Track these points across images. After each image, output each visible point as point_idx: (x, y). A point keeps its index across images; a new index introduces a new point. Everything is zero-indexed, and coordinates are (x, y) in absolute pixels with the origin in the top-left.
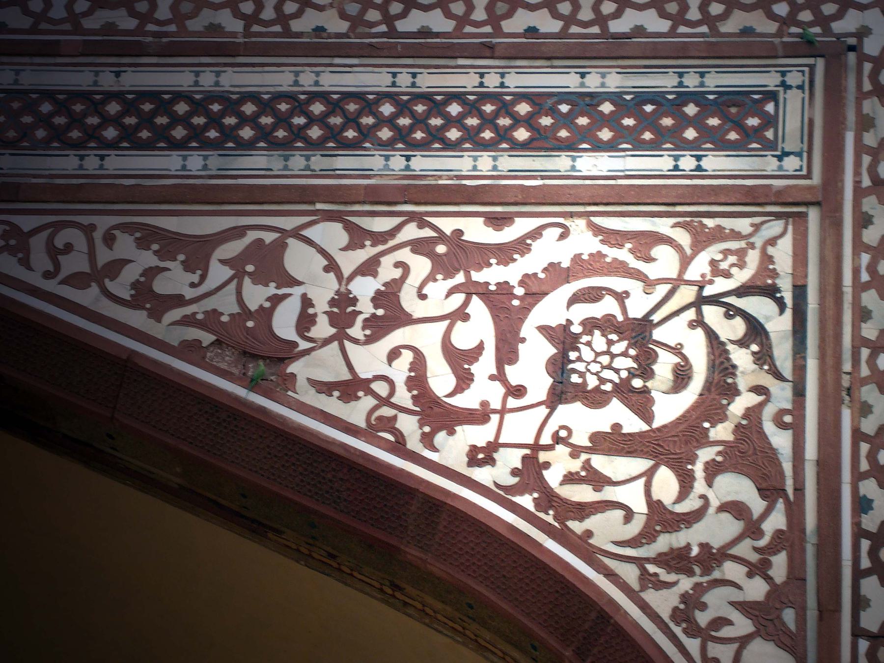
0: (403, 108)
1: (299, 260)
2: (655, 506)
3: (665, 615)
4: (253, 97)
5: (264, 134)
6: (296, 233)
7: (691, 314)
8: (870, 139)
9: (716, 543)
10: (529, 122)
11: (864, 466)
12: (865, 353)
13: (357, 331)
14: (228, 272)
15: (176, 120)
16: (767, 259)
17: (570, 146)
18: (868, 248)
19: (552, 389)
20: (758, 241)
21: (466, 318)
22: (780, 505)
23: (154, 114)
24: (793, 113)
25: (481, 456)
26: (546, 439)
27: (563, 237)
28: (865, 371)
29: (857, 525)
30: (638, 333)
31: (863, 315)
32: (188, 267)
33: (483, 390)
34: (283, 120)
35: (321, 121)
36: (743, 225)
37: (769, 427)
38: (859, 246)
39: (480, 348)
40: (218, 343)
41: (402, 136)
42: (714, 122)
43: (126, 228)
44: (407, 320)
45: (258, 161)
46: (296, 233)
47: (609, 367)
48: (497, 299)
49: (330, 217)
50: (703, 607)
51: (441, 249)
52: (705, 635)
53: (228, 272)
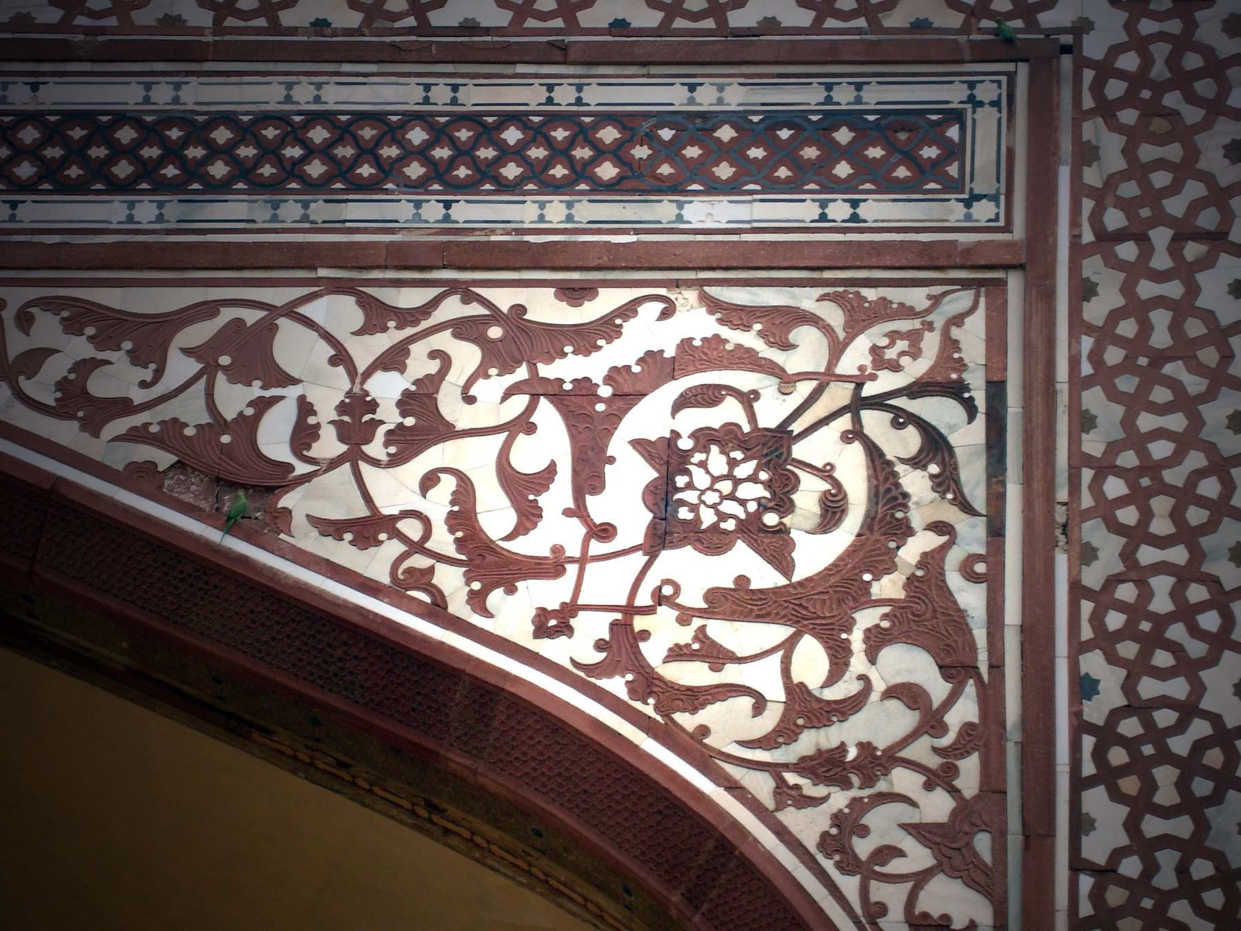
0: (440, 134)
1: (294, 348)
2: (796, 691)
3: (811, 843)
4: (228, 119)
5: (244, 172)
6: (290, 311)
7: (844, 422)
8: (1092, 176)
9: (881, 743)
10: (617, 153)
11: (1087, 633)
12: (1087, 475)
13: (376, 449)
14: (194, 366)
15: (118, 152)
16: (950, 344)
17: (675, 187)
18: (1090, 329)
19: (652, 527)
20: (938, 319)
21: (531, 429)
22: (970, 688)
23: (87, 142)
24: (985, 139)
25: (555, 623)
26: (644, 599)
27: (665, 314)
28: (1087, 501)
29: (1076, 715)
30: (772, 449)
31: (1083, 422)
32: (137, 359)
33: (556, 530)
34: (270, 152)
35: (325, 151)
36: (917, 297)
37: (954, 580)
38: (1078, 326)
39: (551, 470)
40: (180, 466)
41: (439, 174)
42: (875, 152)
43: (48, 304)
44: (448, 432)
45: (235, 208)
46: (290, 311)
47: (732, 497)
48: (575, 402)
49: (338, 287)
50: (864, 831)
51: (495, 332)
52: (866, 870)
53: (194, 366)
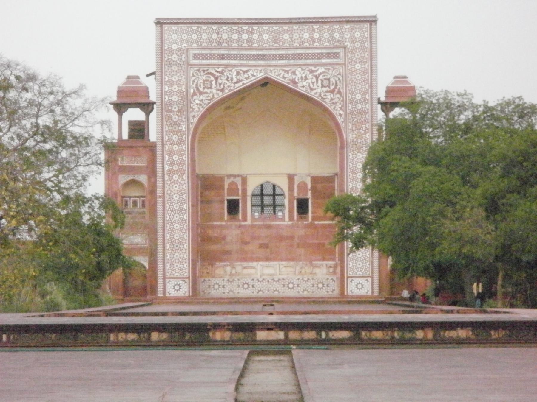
17: (321, 59)
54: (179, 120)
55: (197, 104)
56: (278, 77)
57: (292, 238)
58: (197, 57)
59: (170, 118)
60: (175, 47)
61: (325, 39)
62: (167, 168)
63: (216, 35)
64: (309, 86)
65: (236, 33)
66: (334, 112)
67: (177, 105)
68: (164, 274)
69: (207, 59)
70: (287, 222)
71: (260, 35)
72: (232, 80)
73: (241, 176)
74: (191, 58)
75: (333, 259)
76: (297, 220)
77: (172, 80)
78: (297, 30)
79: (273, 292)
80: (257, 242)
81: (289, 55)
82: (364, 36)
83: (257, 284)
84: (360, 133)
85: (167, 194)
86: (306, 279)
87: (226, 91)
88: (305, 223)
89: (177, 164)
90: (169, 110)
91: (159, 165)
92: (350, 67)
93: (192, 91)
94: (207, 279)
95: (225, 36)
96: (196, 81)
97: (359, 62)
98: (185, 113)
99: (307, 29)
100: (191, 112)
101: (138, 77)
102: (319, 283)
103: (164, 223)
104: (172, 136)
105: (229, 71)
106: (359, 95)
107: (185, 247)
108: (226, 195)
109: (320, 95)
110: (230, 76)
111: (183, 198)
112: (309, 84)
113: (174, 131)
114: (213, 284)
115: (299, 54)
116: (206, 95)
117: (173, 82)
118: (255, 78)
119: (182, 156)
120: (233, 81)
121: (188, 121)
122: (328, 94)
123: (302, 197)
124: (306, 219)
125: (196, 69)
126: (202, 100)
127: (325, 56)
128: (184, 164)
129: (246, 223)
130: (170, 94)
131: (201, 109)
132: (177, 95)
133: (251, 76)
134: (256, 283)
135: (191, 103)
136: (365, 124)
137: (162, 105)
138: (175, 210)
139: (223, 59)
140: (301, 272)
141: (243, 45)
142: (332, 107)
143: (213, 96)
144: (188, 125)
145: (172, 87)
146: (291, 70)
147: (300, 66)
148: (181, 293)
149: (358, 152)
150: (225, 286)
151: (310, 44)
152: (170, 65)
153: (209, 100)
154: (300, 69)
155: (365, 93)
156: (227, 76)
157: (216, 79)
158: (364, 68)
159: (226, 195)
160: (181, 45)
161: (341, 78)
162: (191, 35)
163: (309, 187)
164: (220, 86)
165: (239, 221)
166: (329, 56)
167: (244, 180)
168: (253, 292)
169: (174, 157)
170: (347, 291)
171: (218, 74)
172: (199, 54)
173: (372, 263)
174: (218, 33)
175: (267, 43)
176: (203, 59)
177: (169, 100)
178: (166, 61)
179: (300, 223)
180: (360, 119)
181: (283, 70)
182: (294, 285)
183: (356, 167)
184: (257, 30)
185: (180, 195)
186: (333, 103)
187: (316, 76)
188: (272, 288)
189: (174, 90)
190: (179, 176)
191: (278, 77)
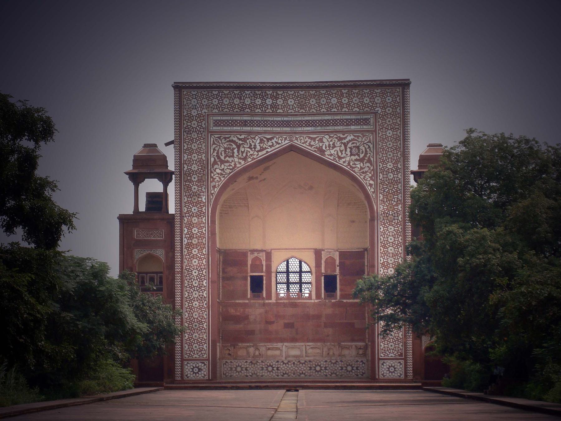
10: (346, 122)
17: (350, 125)
54: (198, 190)
55: (218, 174)
56: (304, 145)
57: (318, 317)
58: (218, 123)
59: (189, 188)
60: (194, 113)
61: (354, 104)
62: (185, 241)
63: (238, 100)
64: (337, 154)
65: (260, 98)
66: (364, 182)
67: (196, 174)
68: (182, 356)
69: (228, 126)
70: (314, 300)
71: (285, 100)
72: (255, 148)
73: (265, 251)
74: (212, 126)
75: (363, 340)
76: (325, 299)
77: (191, 148)
78: (325, 94)
79: (299, 376)
80: (282, 322)
81: (316, 121)
82: (396, 101)
83: (282, 366)
84: (392, 204)
85: (186, 269)
86: (333, 361)
87: (249, 160)
88: (333, 301)
89: (196, 237)
90: (188, 180)
91: (177, 238)
92: (380, 135)
93: (212, 159)
94: (229, 361)
95: (248, 101)
96: (217, 149)
97: (391, 129)
98: (205, 183)
99: (336, 94)
100: (211, 182)
101: (155, 146)
102: (347, 365)
103: (182, 300)
104: (191, 208)
105: (252, 138)
106: (391, 164)
107: (205, 326)
108: (249, 271)
109: (349, 164)
110: (253, 144)
111: (202, 274)
112: (337, 152)
113: (193, 203)
114: (235, 366)
115: (326, 120)
116: (227, 164)
117: (193, 150)
118: (280, 145)
119: (202, 229)
120: (256, 150)
121: (208, 192)
122: (357, 163)
123: (329, 273)
124: (334, 297)
125: (216, 136)
126: (223, 170)
127: (354, 122)
128: (204, 237)
129: (270, 301)
130: (190, 162)
131: (222, 179)
132: (196, 164)
133: (275, 144)
134: (282, 366)
135: (211, 172)
136: (397, 195)
137: (181, 175)
138: (194, 287)
139: (245, 125)
140: (328, 354)
141: (267, 111)
142: (362, 177)
143: (235, 164)
144: (208, 195)
145: (191, 155)
146: (318, 137)
147: (327, 133)
148: (200, 376)
149: (389, 225)
150: (248, 369)
151: (338, 110)
152: (189, 132)
153: (231, 169)
154: (327, 137)
155: (397, 162)
156: (250, 144)
157: (238, 147)
158: (396, 135)
159: (249, 271)
160: (201, 111)
161: (371, 146)
162: (212, 100)
163: (337, 262)
164: (242, 155)
165: (263, 299)
166: (357, 122)
167: (269, 255)
168: (278, 376)
169: (193, 230)
170: (379, 375)
171: (241, 142)
172: (220, 121)
173: (405, 345)
174: (240, 99)
175: (293, 109)
176: (224, 126)
177: (188, 169)
178: (185, 128)
179: (327, 301)
180: (392, 190)
181: (309, 138)
182: (321, 367)
183: (387, 241)
184: (282, 95)
185: (199, 271)
186: (363, 173)
187: (344, 144)
188: (298, 371)
189: (194, 159)
190: (198, 250)
191: (304, 145)
